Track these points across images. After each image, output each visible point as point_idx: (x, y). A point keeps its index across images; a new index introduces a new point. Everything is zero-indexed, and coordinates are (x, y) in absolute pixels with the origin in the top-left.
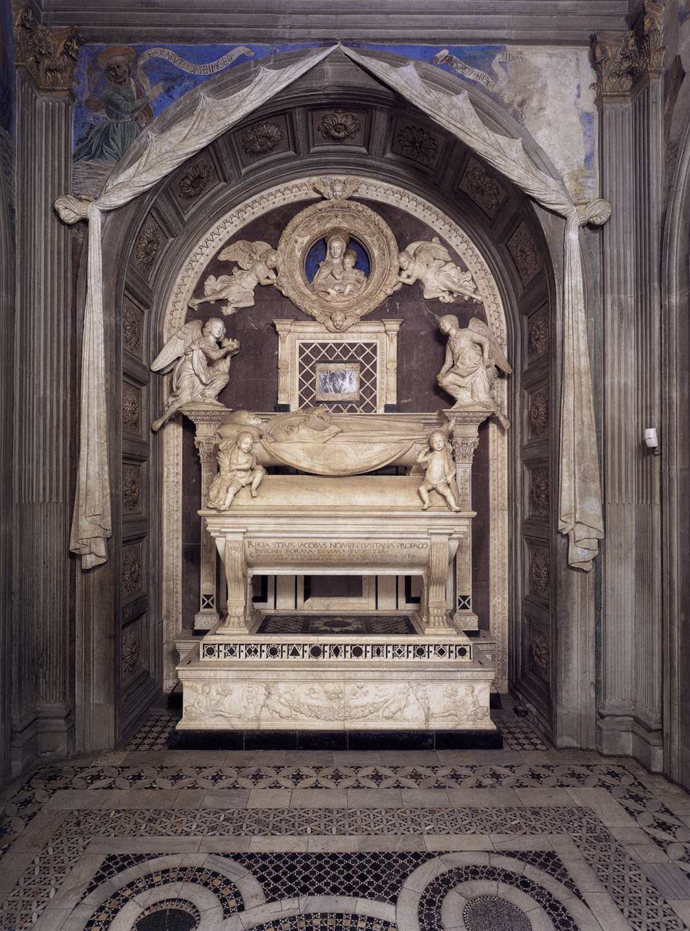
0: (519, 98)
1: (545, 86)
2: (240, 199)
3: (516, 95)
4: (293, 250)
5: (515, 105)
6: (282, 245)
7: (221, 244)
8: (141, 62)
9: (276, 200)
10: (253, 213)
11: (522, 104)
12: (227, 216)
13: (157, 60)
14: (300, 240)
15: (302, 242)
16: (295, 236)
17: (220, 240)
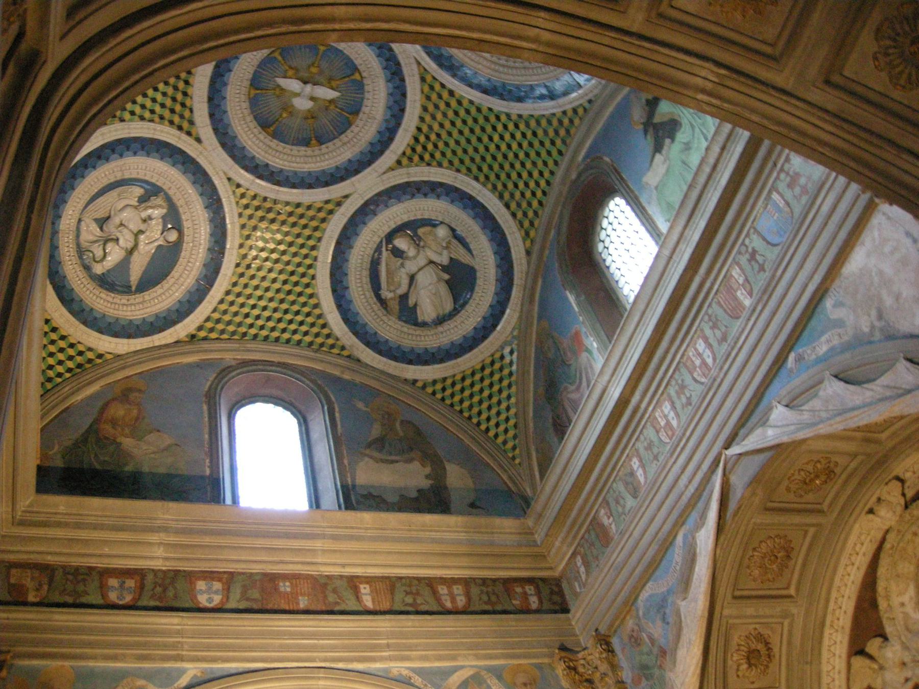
0: (874, 313)
1: (881, 273)
2: (820, 613)
3: (869, 315)
4: (906, 615)
5: (877, 324)
6: (889, 629)
7: (843, 675)
8: (641, 613)
9: (852, 578)
10: (845, 612)
11: (880, 317)
12: (826, 642)
13: (647, 600)
14: (906, 598)
15: (911, 598)
16: (896, 601)
17: (839, 672)
